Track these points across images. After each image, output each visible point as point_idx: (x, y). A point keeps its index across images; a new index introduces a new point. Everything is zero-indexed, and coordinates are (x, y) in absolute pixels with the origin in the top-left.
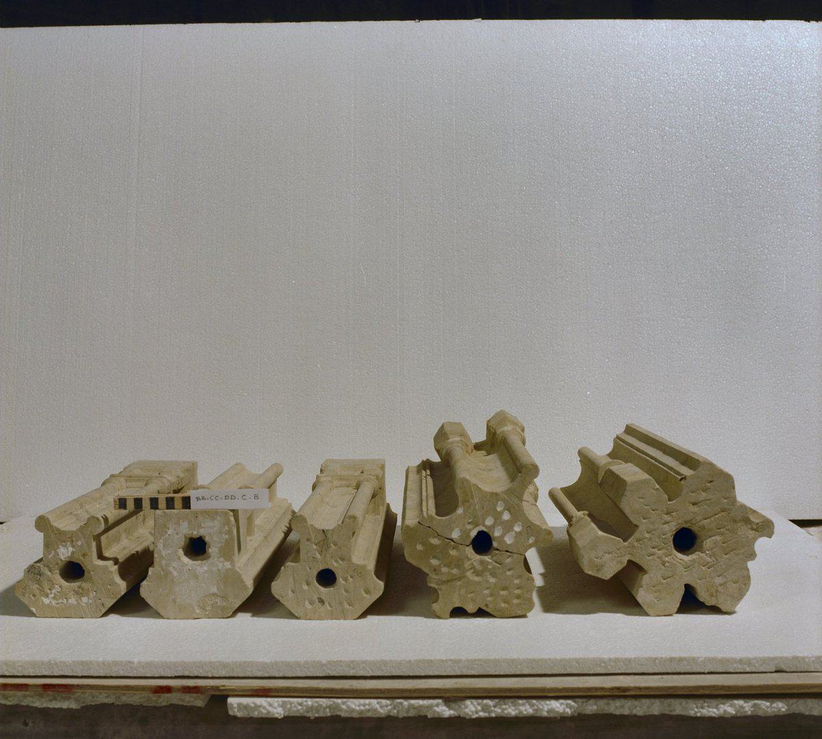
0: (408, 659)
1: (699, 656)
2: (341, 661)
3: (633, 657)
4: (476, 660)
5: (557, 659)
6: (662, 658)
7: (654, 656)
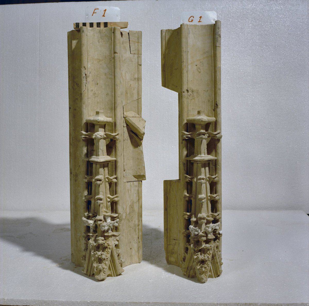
0: (126, 302)
1: (258, 302)
2: (96, 302)
3: (228, 303)
4: (157, 303)
5: (193, 303)
6: (241, 303)
7: (238, 303)
